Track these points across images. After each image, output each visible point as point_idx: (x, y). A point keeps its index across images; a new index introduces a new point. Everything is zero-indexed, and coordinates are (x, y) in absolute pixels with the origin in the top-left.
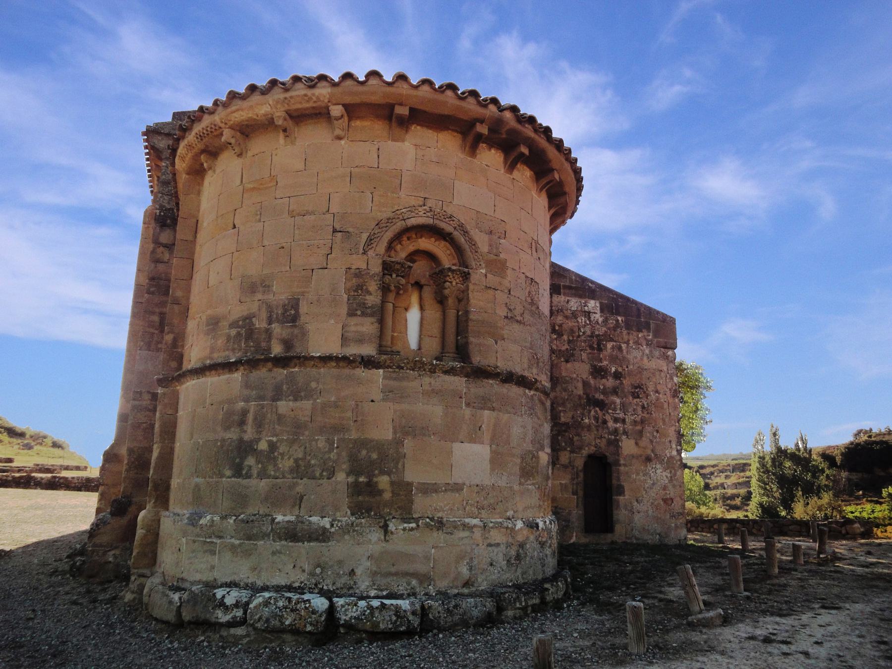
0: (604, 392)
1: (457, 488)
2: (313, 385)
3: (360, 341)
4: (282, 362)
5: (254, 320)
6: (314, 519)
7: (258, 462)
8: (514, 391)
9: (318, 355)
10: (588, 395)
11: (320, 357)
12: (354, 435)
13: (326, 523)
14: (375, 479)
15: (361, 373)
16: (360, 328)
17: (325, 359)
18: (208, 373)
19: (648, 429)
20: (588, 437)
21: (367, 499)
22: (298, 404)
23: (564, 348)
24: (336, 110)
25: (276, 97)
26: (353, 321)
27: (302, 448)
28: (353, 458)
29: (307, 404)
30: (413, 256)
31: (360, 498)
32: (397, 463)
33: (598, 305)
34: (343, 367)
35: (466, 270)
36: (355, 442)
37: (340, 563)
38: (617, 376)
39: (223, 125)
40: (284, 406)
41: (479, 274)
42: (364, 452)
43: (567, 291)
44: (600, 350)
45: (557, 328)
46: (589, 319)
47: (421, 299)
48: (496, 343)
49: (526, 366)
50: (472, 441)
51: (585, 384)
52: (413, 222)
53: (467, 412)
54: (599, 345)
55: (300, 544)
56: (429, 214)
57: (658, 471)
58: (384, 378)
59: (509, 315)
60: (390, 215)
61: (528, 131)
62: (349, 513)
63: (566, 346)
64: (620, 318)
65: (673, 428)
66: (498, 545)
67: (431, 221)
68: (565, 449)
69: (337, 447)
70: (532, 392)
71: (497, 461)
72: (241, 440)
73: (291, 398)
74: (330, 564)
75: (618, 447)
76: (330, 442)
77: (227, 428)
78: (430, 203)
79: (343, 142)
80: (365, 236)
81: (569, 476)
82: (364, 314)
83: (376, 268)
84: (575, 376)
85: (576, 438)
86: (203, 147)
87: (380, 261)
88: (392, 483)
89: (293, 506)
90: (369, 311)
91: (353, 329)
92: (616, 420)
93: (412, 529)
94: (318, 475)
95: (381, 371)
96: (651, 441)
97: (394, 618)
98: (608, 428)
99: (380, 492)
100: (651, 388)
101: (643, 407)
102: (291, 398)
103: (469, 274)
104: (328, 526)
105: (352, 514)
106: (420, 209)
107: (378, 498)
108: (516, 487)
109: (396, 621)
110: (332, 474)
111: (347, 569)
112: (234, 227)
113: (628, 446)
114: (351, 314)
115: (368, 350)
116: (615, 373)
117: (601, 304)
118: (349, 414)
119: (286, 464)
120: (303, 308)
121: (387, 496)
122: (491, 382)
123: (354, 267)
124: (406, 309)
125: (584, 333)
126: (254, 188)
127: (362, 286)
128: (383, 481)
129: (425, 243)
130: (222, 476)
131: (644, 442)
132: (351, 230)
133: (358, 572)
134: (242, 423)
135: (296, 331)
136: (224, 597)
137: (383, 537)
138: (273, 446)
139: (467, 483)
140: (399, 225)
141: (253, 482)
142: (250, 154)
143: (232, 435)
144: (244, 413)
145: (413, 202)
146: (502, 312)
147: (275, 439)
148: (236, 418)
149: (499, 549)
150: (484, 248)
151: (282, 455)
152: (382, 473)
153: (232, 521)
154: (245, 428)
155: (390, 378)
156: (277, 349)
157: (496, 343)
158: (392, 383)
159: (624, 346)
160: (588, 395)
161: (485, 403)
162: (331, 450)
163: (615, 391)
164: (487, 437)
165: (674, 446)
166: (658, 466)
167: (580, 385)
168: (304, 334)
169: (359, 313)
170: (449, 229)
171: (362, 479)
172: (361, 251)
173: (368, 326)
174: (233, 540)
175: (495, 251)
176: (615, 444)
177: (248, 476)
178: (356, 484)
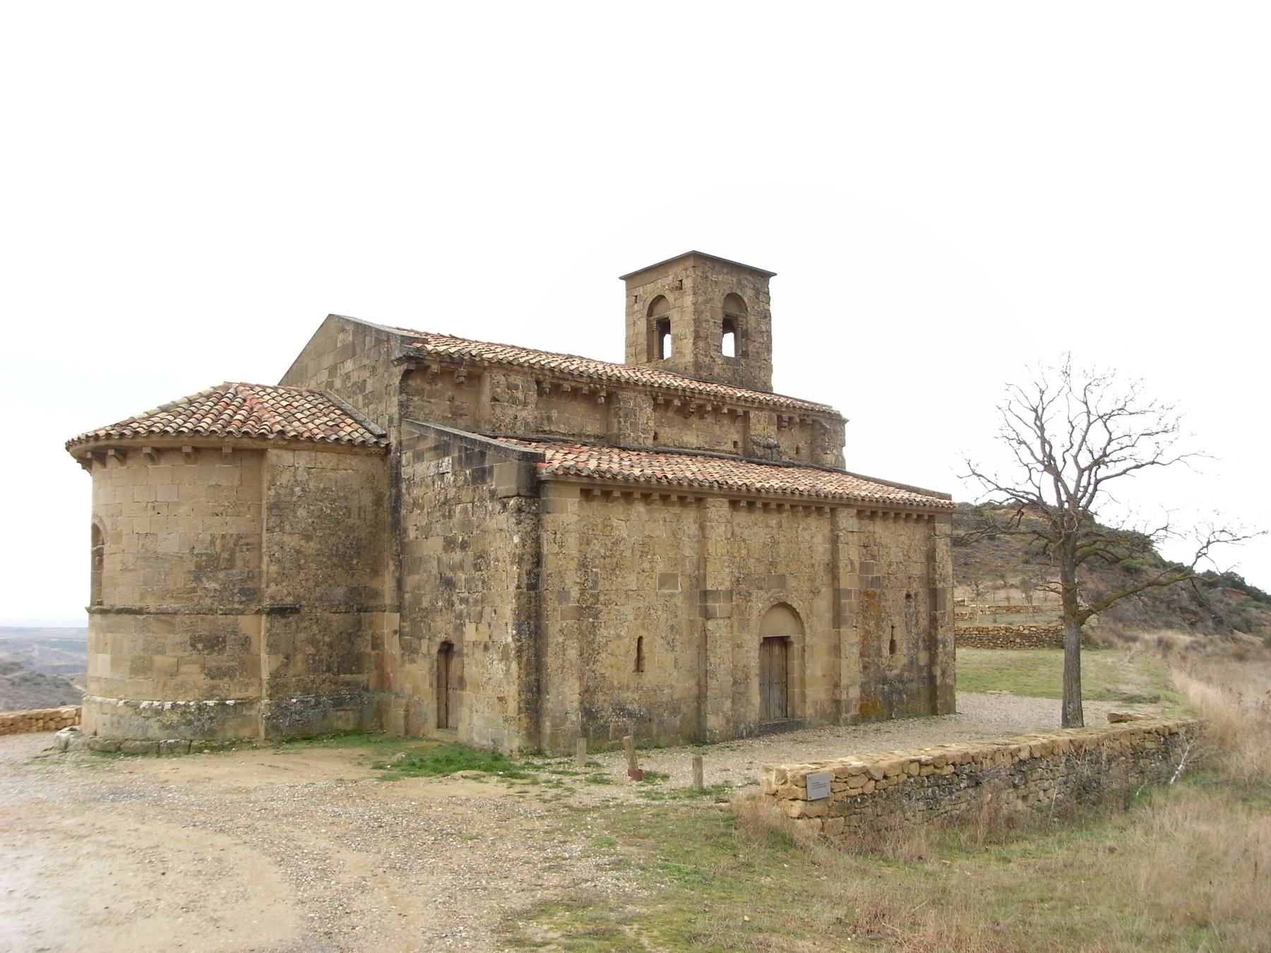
0: (453, 568)
19: (488, 610)
44: (450, 517)
71: (115, 664)
75: (463, 633)
92: (462, 600)
101: (484, 582)
113: (470, 632)
131: (483, 628)
150: (109, 528)
163: (461, 567)
166: (495, 657)
167: (435, 563)
176: (459, 628)
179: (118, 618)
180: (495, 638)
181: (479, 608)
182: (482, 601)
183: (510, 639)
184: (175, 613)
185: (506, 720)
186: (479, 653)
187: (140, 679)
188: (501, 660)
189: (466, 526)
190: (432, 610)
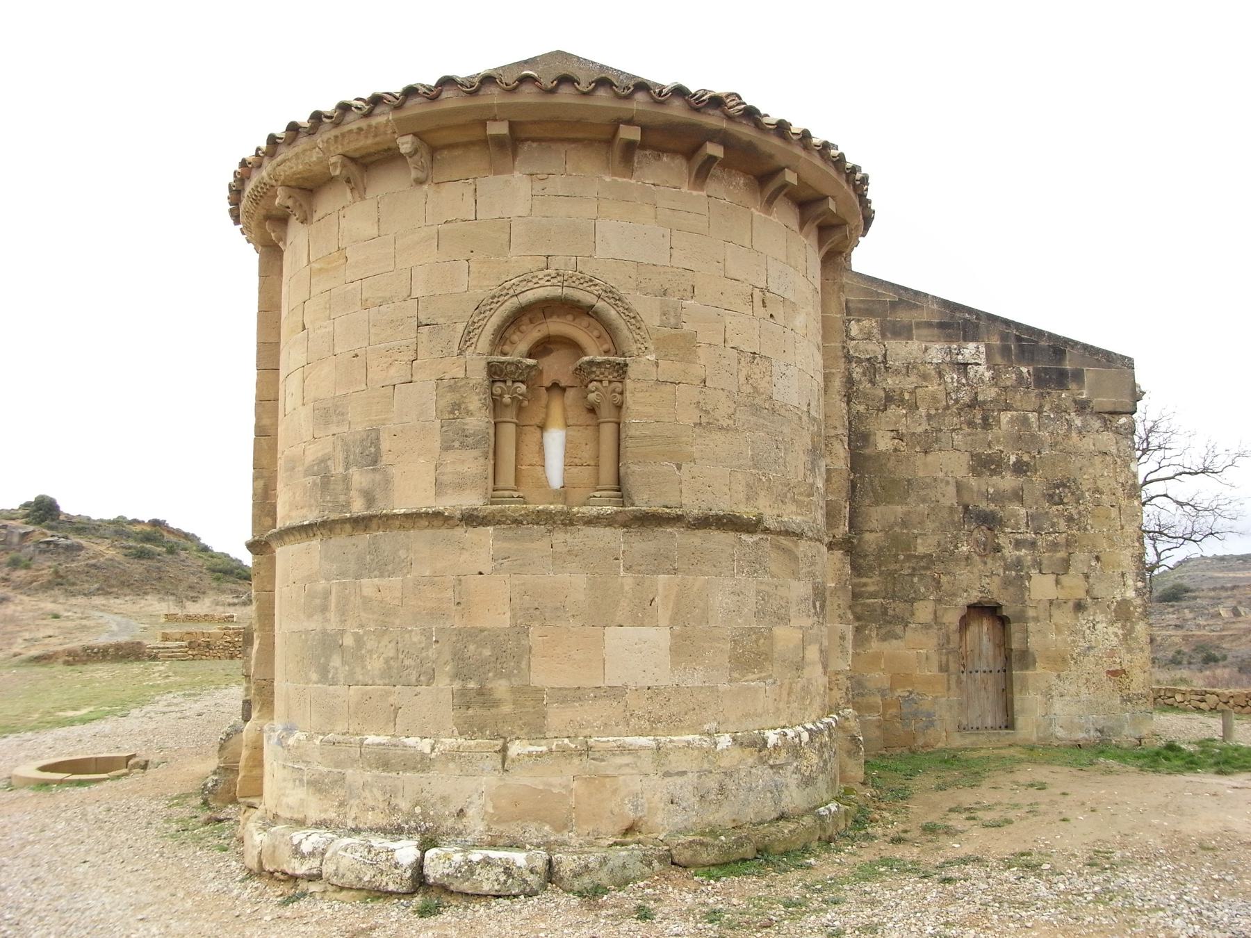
0: (999, 498)
1: (616, 693)
2: (402, 554)
3: (460, 486)
4: (361, 523)
5: (329, 463)
6: (411, 741)
7: (344, 663)
8: (721, 539)
9: (402, 511)
10: (966, 508)
11: (406, 515)
12: (458, 624)
13: (425, 746)
14: (490, 686)
15: (459, 532)
16: (459, 468)
17: (413, 518)
18: (286, 539)
20: (963, 575)
21: (480, 712)
22: (385, 582)
23: (920, 430)
24: (405, 144)
25: (325, 137)
26: (450, 457)
27: (393, 644)
28: (458, 657)
29: (396, 580)
30: (542, 348)
31: (470, 712)
32: (519, 662)
33: (982, 349)
34: (439, 528)
35: (620, 359)
36: (459, 632)
37: (445, 799)
38: (1020, 468)
39: (273, 182)
40: (368, 585)
41: (642, 364)
42: (472, 647)
43: (925, 332)
45: (907, 396)
46: (966, 374)
47: (564, 410)
48: (679, 467)
49: (742, 496)
50: (637, 622)
51: (959, 487)
52: (530, 296)
53: (628, 580)
54: (985, 419)
55: (394, 774)
56: (555, 281)
57: (1098, 626)
58: (496, 538)
59: (704, 420)
60: (496, 291)
61: (713, 120)
62: (456, 732)
63: (925, 426)
64: (1024, 370)
65: (1128, 552)
66: (684, 773)
67: (558, 292)
68: (925, 598)
69: (437, 641)
70: (756, 538)
71: (683, 649)
72: (324, 632)
73: (376, 573)
74: (432, 801)
75: (1023, 589)
76: (426, 633)
77: (310, 616)
78: (555, 263)
79: (425, 187)
80: (460, 328)
81: (935, 641)
82: (464, 446)
83: (479, 375)
84: (941, 475)
85: (944, 579)
86: (263, 212)
87: (483, 364)
88: (513, 690)
89: (387, 724)
90: (470, 440)
91: (449, 469)
92: (1018, 544)
93: (540, 755)
94: (413, 679)
95: (490, 529)
96: (1087, 577)
97: (502, 878)
98: (1003, 558)
99: (496, 703)
100: (1086, 485)
101: (1070, 519)
102: (376, 573)
103: (626, 365)
104: (427, 750)
105: (461, 734)
106: (541, 275)
107: (494, 711)
108: (723, 687)
109: (505, 882)
110: (431, 678)
111: (454, 809)
112: (304, 328)
113: (1041, 587)
114: (446, 448)
115: (472, 500)
116: (1014, 464)
117: (988, 347)
118: (450, 594)
119: (375, 665)
120: (385, 445)
121: (507, 708)
122: (669, 530)
123: (447, 376)
124: (542, 428)
125: (957, 401)
126: (320, 270)
127: (459, 405)
128: (500, 687)
129: (557, 326)
130: (308, 681)
132: (441, 321)
133: (471, 812)
134: (324, 609)
135: (378, 477)
136: (300, 843)
137: (500, 766)
138: (359, 640)
139: (631, 685)
140: (510, 305)
141: (340, 689)
142: (315, 218)
143: (315, 624)
144: (327, 594)
145: (529, 264)
146: (689, 417)
147: (361, 632)
148: (318, 601)
149: (685, 778)
151: (370, 652)
152: (499, 675)
153: (318, 742)
154: (327, 614)
155: (506, 539)
156: (358, 508)
157: (679, 467)
158: (506, 545)
159: (1033, 417)
160: (966, 508)
161: (661, 563)
162: (427, 648)
163: (1018, 496)
164: (664, 615)
165: (1130, 582)
166: (1099, 617)
167: (951, 490)
168: (387, 481)
169: (457, 444)
170: (587, 298)
171: (472, 685)
172: (456, 351)
173: (471, 463)
174: (320, 767)
175: (673, 321)
177: (334, 683)
178: (464, 692)
179: (696, 539)
180: (1099, 590)
181: (1062, 554)
182: (1068, 544)
183: (1131, 594)
184: (800, 535)
185: (1127, 699)
186: (1063, 617)
187: (751, 680)
188: (1112, 623)
189: (1023, 438)
190: (946, 556)
